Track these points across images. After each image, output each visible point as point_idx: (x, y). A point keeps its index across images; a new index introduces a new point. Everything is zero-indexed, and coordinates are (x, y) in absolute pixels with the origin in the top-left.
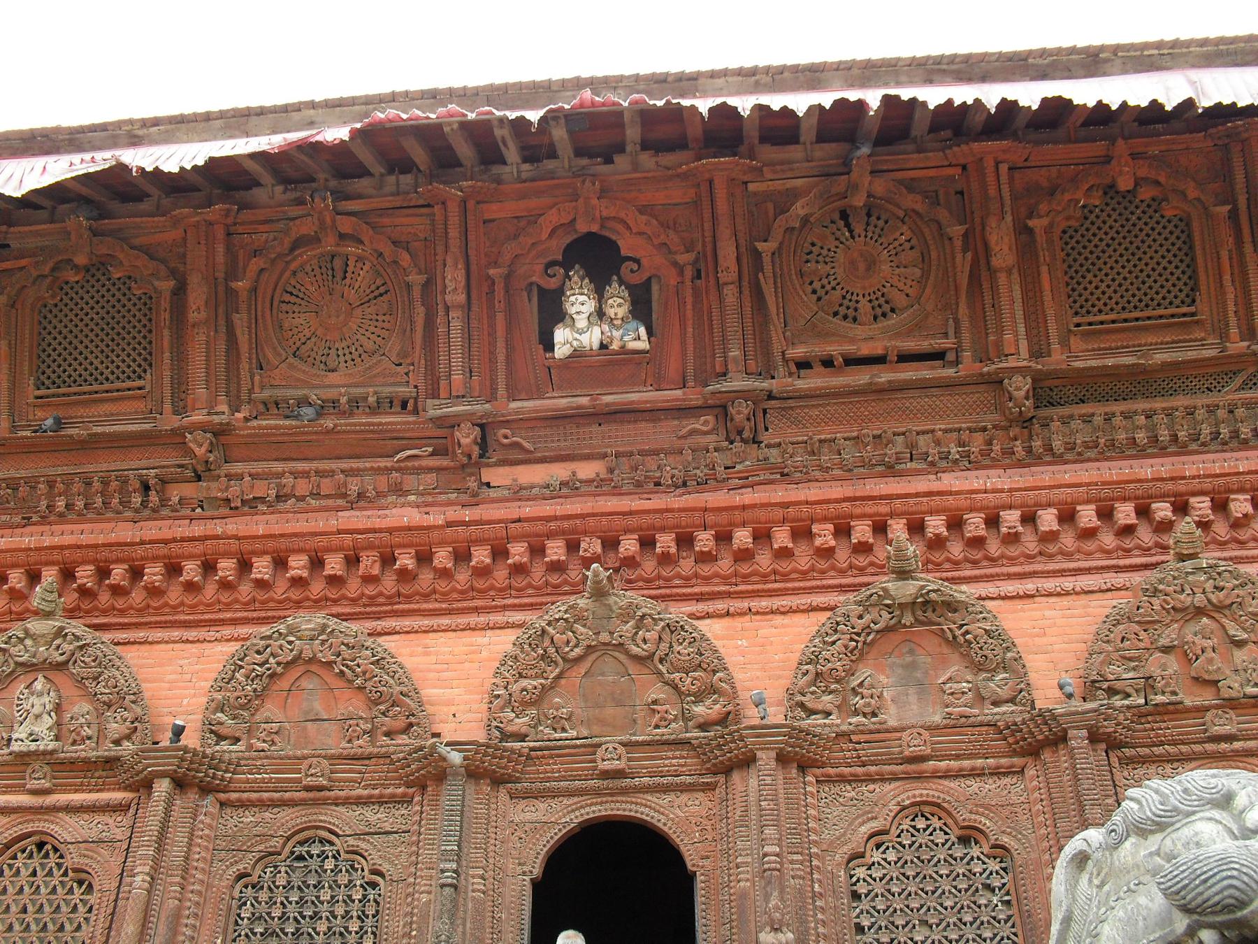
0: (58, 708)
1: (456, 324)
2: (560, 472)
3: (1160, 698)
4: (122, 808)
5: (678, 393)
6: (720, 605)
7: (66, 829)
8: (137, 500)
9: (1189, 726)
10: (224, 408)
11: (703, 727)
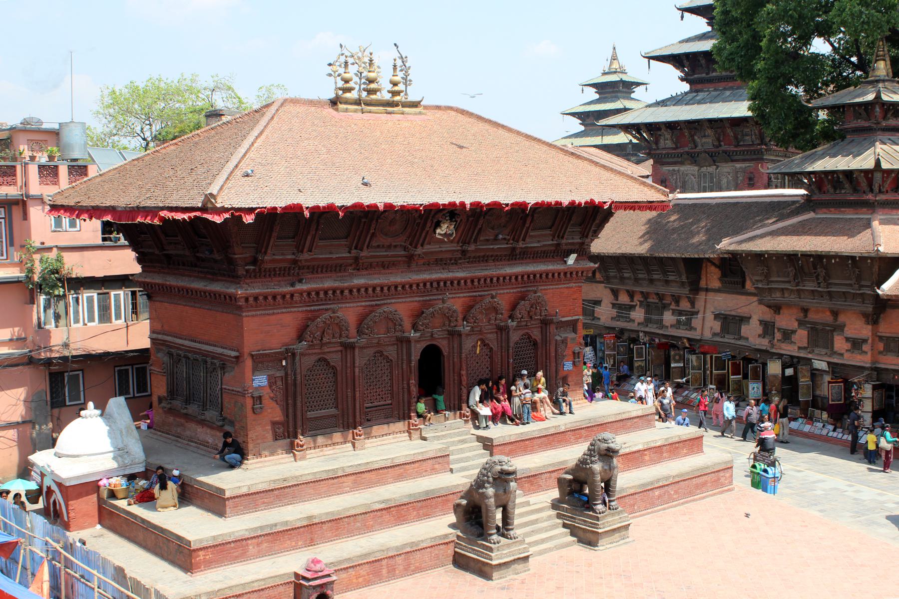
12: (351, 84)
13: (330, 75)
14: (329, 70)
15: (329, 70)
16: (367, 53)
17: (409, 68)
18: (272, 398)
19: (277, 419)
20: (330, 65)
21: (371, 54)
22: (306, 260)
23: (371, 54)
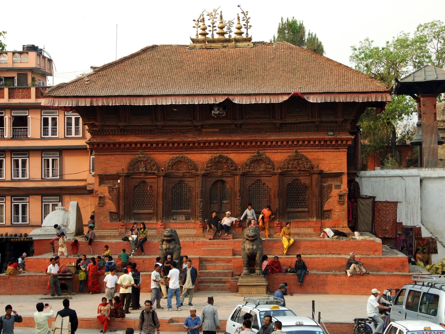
0: (145, 166)
1: (198, 114)
2: (213, 130)
3: (289, 170)
4: (155, 178)
5: (229, 121)
6: (235, 152)
7: (148, 180)
8: (149, 132)
9: (292, 173)
10: (163, 121)
11: (232, 170)
12: (207, 31)
13: (194, 27)
14: (194, 24)
15: (194, 24)
16: (218, 12)
17: (249, 18)
18: (110, 199)
19: (113, 211)
20: (194, 20)
21: (221, 12)
22: (125, 126)
23: (221, 12)
